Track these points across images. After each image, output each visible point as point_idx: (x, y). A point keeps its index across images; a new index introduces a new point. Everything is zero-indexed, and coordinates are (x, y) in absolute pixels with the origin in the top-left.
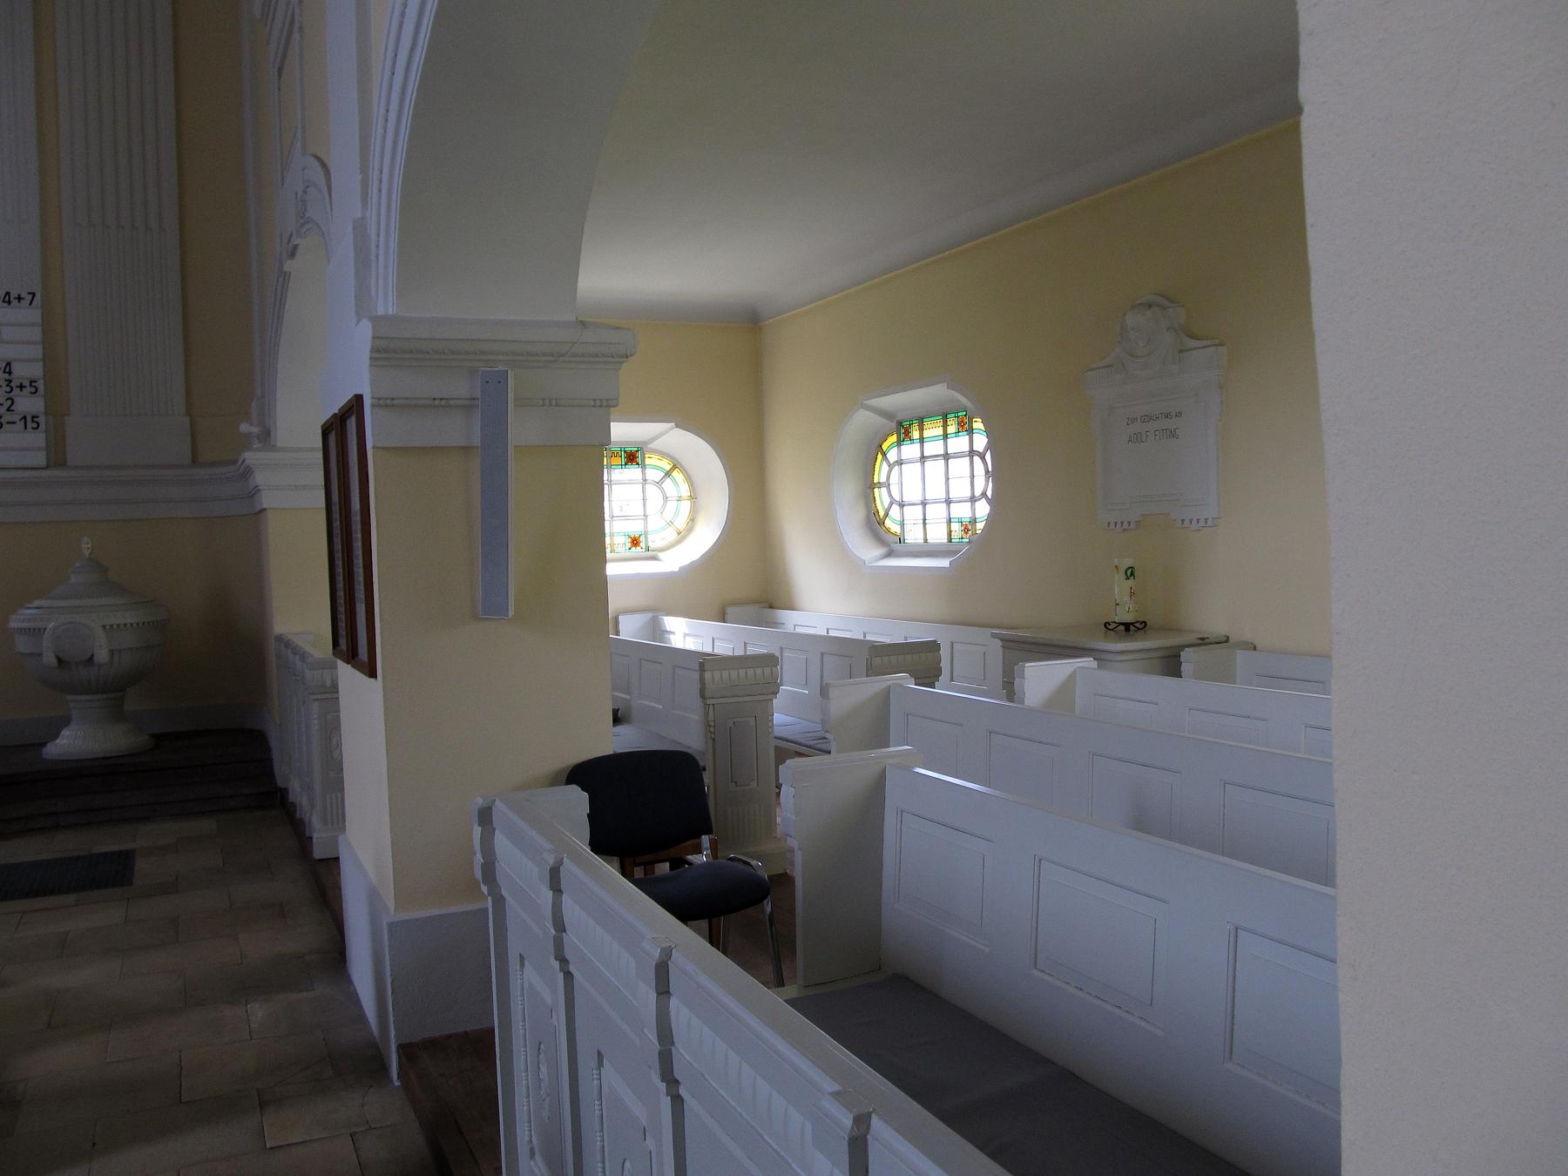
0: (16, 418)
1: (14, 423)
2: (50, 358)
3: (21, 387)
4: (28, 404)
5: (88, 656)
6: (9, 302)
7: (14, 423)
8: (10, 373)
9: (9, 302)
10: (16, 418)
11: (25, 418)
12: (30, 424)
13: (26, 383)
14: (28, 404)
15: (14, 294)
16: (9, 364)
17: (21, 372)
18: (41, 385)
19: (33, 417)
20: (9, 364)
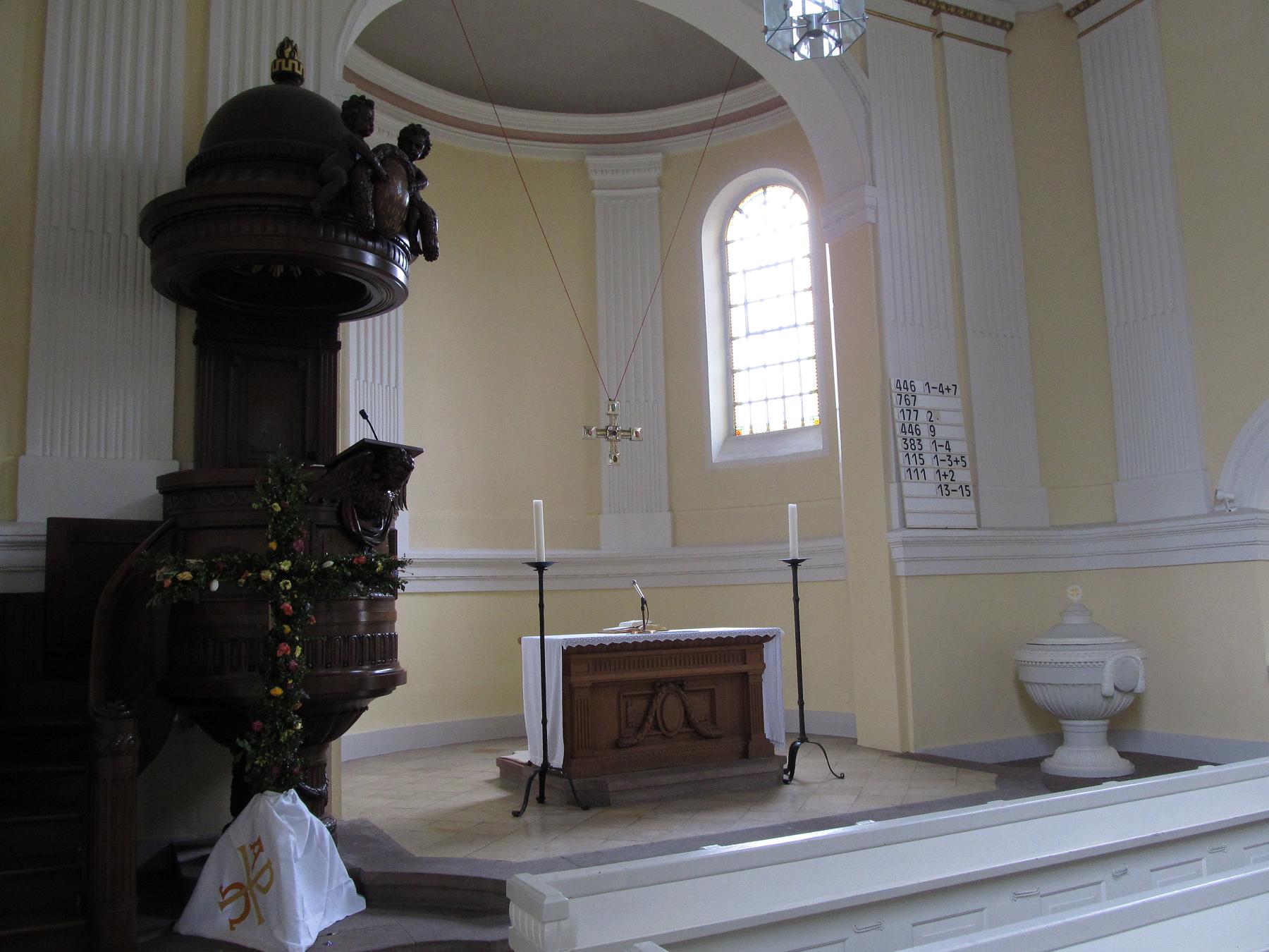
0: (957, 487)
1: (956, 491)
2: (971, 441)
3: (957, 461)
4: (962, 476)
5: (1131, 689)
6: (943, 392)
7: (956, 491)
8: (949, 449)
9: (943, 392)
10: (957, 487)
11: (961, 486)
12: (966, 493)
13: (959, 459)
14: (962, 476)
15: (945, 387)
16: (947, 442)
17: (958, 448)
18: (966, 459)
19: (966, 486)
20: (947, 442)
